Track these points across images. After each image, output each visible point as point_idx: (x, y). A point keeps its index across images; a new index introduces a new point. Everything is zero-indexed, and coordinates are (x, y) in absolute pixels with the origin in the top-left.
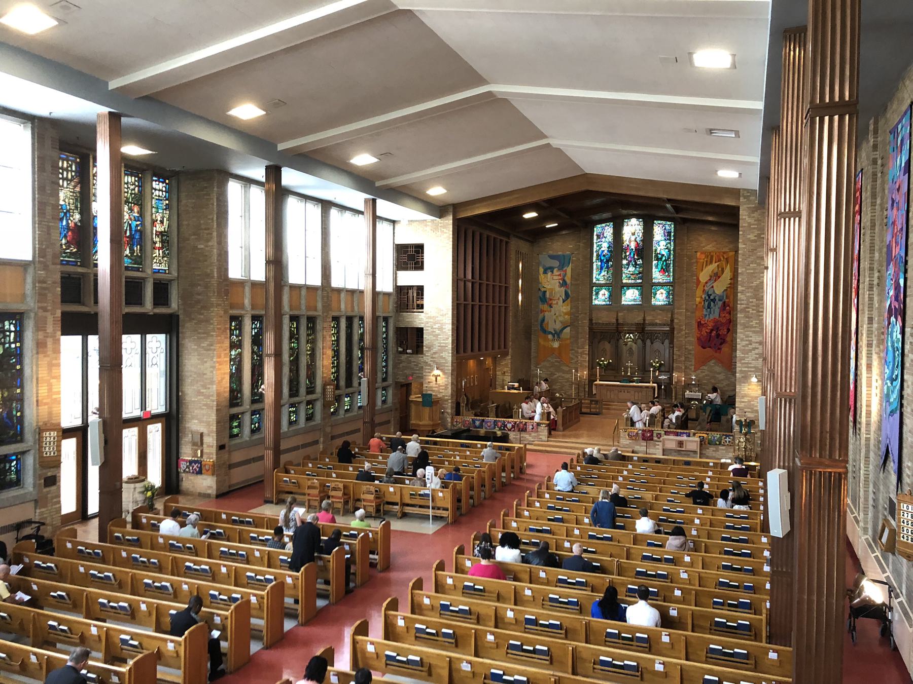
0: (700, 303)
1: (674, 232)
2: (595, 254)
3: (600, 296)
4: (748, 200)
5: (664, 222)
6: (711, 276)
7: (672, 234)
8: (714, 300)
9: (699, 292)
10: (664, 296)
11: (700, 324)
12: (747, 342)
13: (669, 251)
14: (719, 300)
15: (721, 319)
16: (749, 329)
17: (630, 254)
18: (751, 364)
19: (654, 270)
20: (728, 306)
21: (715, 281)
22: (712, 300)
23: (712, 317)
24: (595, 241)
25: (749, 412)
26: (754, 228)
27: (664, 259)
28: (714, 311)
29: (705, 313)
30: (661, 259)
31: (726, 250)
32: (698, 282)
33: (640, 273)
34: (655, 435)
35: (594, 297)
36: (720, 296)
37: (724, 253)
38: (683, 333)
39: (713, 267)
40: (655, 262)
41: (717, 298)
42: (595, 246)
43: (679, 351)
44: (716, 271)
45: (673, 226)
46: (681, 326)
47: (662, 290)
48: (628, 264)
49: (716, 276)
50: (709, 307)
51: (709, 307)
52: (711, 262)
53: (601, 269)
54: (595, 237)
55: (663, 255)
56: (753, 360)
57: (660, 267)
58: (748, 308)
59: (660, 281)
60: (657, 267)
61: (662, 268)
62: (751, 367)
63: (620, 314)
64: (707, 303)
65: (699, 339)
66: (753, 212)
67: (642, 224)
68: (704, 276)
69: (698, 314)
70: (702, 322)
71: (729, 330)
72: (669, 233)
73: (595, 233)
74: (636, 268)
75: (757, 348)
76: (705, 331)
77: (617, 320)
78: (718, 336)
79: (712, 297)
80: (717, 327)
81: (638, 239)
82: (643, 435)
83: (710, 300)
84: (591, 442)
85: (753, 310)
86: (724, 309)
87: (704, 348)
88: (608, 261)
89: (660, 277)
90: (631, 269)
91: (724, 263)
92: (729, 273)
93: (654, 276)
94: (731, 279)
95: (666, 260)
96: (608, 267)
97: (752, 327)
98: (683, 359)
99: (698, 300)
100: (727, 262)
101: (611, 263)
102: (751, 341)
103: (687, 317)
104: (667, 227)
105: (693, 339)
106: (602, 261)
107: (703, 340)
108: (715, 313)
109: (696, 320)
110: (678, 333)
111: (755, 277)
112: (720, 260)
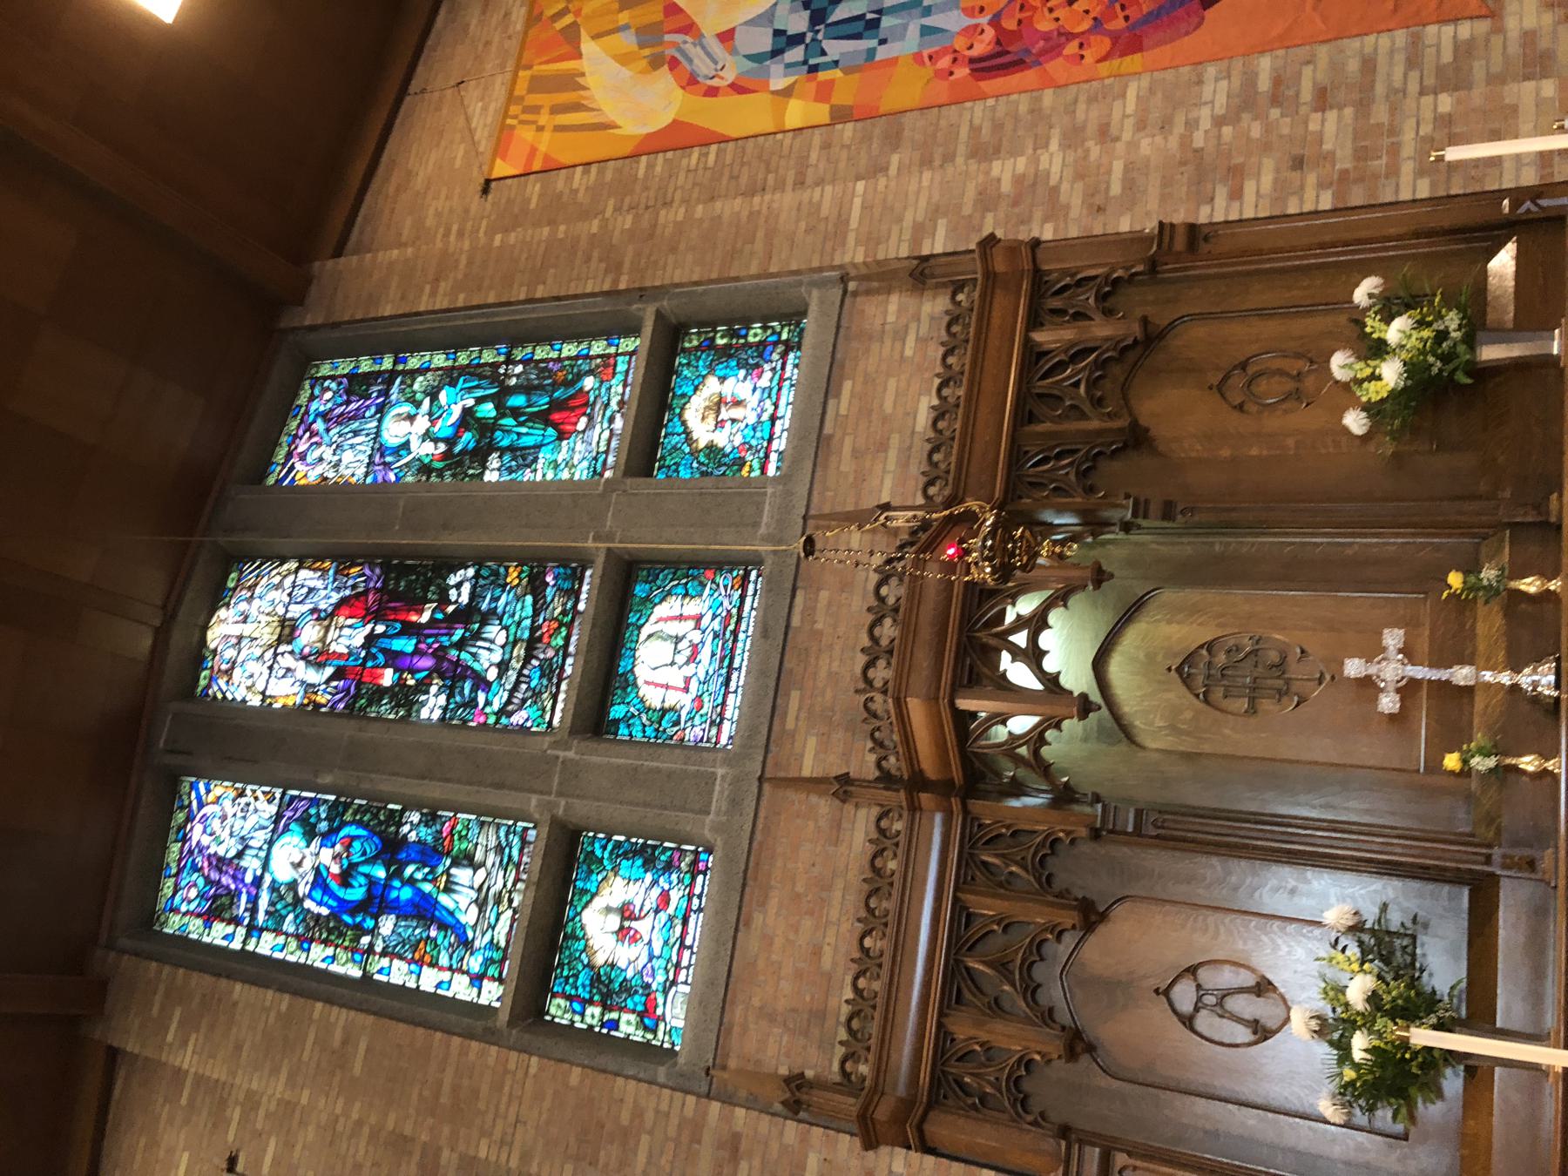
0: (824, 93)
1: (354, 352)
2: (318, 955)
3: (627, 957)
6: (655, 63)
7: (366, 365)
10: (737, 385)
13: (450, 376)
17: (394, 658)
19: (541, 472)
22: (817, 18)
27: (487, 410)
30: (486, 429)
33: (536, 587)
35: (628, 1027)
38: (1054, 161)
42: (266, 945)
43: (1236, 176)
44: (627, 41)
47: (692, 414)
48: (454, 675)
53: (424, 911)
54: (218, 934)
57: (530, 436)
60: (524, 456)
61: (543, 418)
63: (808, 768)
64: (835, 48)
72: (356, 385)
73: (195, 929)
74: (485, 619)
88: (392, 850)
93: (582, 473)
95: (499, 400)
101: (413, 829)
106: (377, 902)
109: (958, 99)
110: (1055, 209)
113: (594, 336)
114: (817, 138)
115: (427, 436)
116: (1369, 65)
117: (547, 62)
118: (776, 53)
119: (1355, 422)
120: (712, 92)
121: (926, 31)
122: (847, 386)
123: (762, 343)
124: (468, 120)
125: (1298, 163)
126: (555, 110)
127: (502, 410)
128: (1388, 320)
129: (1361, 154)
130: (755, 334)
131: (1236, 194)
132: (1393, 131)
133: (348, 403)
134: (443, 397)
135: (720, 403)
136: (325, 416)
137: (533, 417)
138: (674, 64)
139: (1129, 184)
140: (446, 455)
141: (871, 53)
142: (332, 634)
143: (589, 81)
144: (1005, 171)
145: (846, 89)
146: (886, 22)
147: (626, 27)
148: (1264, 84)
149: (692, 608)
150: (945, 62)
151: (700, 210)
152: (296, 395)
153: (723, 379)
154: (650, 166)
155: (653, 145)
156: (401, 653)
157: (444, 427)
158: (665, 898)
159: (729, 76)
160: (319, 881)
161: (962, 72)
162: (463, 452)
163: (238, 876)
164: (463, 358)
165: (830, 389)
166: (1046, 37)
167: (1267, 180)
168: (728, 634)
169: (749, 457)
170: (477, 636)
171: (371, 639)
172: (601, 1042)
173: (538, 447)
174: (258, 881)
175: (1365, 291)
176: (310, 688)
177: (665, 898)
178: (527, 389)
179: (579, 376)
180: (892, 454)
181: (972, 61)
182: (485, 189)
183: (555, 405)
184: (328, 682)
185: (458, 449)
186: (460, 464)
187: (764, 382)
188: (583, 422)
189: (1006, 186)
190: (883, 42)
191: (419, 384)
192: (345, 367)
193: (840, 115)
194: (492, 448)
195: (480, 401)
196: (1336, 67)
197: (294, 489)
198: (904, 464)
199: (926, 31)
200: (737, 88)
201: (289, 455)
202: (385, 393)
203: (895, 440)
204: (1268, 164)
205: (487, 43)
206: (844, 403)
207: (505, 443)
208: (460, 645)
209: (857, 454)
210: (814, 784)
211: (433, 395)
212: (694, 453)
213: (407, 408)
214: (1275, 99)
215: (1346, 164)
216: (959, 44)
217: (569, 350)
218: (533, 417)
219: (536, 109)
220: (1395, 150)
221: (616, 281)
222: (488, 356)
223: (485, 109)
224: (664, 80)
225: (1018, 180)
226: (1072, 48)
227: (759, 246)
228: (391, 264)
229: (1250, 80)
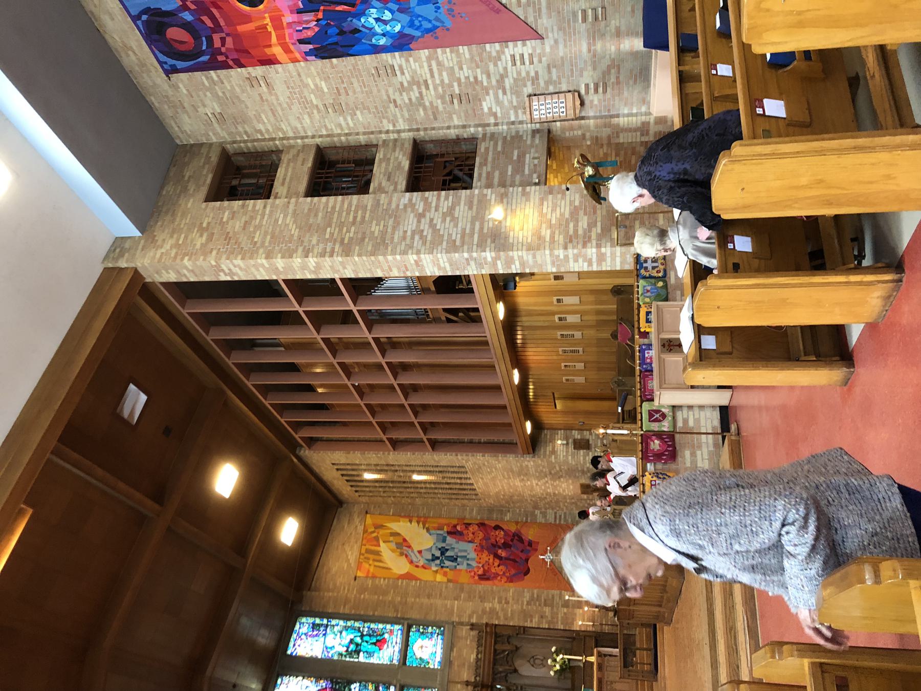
0: (445, 574)
1: (315, 617)
4: (129, 250)
5: (294, 636)
6: (401, 554)
8: (443, 551)
9: (426, 575)
12: (417, 237)
14: (444, 540)
15: (477, 540)
16: (388, 236)
18: (464, 230)
19: (374, 660)
20: (455, 526)
21: (409, 547)
22: (442, 554)
23: (473, 555)
25: (576, 226)
26: (186, 238)
27: (358, 640)
28: (461, 551)
29: (463, 567)
30: (357, 645)
31: (361, 529)
32: (408, 576)
34: (655, 427)
36: (438, 540)
37: (365, 531)
38: (497, 606)
39: (386, 550)
40: (362, 658)
41: (440, 545)
43: (531, 617)
44: (393, 546)
45: (304, 620)
46: (484, 612)
49: (403, 546)
50: (454, 559)
51: (454, 559)
52: (378, 553)
55: (351, 641)
56: (456, 226)
58: (342, 240)
59: (397, 649)
60: (370, 654)
61: (375, 644)
62: (473, 229)
64: (447, 563)
65: (511, 580)
66: (153, 240)
67: (286, 679)
68: (398, 565)
69: (464, 578)
70: (480, 572)
71: (497, 527)
72: (315, 626)
75: (432, 220)
76: (497, 568)
78: (506, 546)
79: (438, 554)
80: (492, 548)
82: (658, 456)
83: (442, 556)
84: (704, 606)
85: (348, 231)
86: (461, 534)
87: (527, 572)
89: (390, 650)
91: (382, 532)
92: (401, 523)
93: (386, 661)
94: (411, 521)
95: (362, 636)
97: (383, 233)
98: (547, 610)
99: (439, 578)
102: (413, 233)
103: (470, 598)
104: (304, 630)
105: (511, 590)
107: (513, 572)
108: (467, 549)
109: (476, 583)
110: (498, 618)
111: (281, 231)
112: (377, 539)
113: (387, 623)
114: (444, 585)
116: (553, 596)
117: (372, 545)
118: (433, 560)
119: (552, 673)
120: (417, 566)
121: (468, 565)
122: (455, 649)
123: (432, 633)
124: (347, 556)
125: (542, 617)
126: (374, 560)
127: (363, 641)
128: (557, 655)
129: (553, 618)
130: (430, 629)
131: (531, 621)
132: (558, 614)
134: (344, 633)
135: (422, 647)
136: (306, 634)
137: (372, 644)
138: (406, 556)
139: (512, 614)
140: (347, 651)
141: (456, 567)
143: (383, 554)
144: (488, 606)
145: (451, 574)
146: (459, 559)
147: (391, 542)
148: (535, 596)
150: (472, 574)
151: (418, 600)
154: (402, 583)
157: (346, 641)
159: (421, 563)
161: (477, 578)
162: (352, 651)
164: (349, 623)
165: (451, 650)
166: (494, 574)
167: (537, 619)
169: (430, 661)
173: (374, 652)
175: (553, 649)
178: (370, 636)
179: (383, 634)
180: (466, 667)
181: (479, 575)
182: (355, 579)
183: (378, 641)
185: (350, 650)
186: (351, 654)
188: (386, 646)
189: (488, 609)
191: (336, 629)
192: (311, 620)
193: (449, 581)
194: (360, 651)
196: (548, 595)
197: (296, 656)
198: (468, 669)
199: (468, 565)
200: (424, 567)
201: (294, 645)
202: (326, 630)
203: (467, 664)
204: (537, 616)
205: (351, 534)
206: (454, 654)
207: (364, 650)
209: (458, 666)
211: (341, 633)
212: (417, 659)
213: (333, 636)
214: (537, 600)
215: (550, 619)
217: (381, 626)
218: (372, 644)
219: (368, 559)
220: (558, 618)
221: (397, 614)
222: (357, 624)
223: (352, 554)
224: (403, 560)
225: (490, 608)
226: (499, 578)
227: (433, 611)
228: (330, 597)
229: (533, 594)
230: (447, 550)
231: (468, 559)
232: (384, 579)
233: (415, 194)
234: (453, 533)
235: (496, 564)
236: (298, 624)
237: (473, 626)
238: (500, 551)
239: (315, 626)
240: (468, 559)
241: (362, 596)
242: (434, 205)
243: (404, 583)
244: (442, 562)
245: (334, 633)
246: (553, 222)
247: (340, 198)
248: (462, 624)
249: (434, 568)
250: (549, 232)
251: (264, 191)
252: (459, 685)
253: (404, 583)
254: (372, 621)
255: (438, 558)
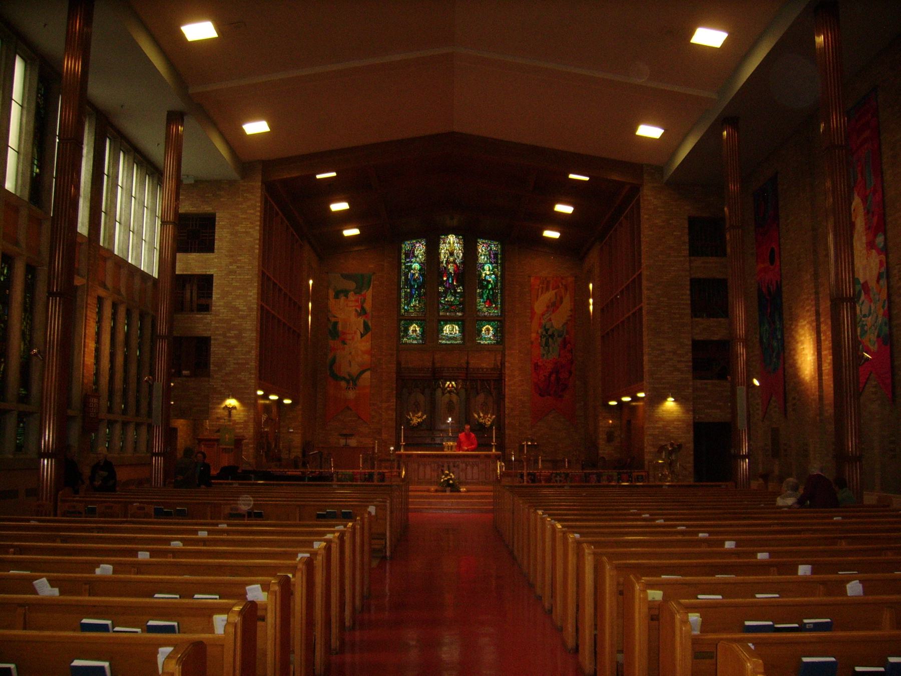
0: (537, 339)
6: (548, 307)
7: (499, 256)
8: (552, 336)
11: (536, 366)
13: (496, 276)
14: (559, 336)
17: (448, 279)
21: (553, 311)
22: (550, 336)
24: (403, 261)
27: (490, 286)
30: (487, 286)
32: (533, 313)
35: (402, 334)
39: (549, 295)
45: (499, 247)
48: (445, 292)
49: (554, 306)
50: (547, 344)
52: (547, 289)
53: (412, 296)
54: (403, 256)
55: (489, 282)
61: (488, 298)
64: (544, 340)
68: (539, 306)
70: (539, 364)
72: (496, 255)
74: (455, 297)
77: (433, 363)
81: (458, 261)
90: (450, 298)
91: (563, 291)
94: (571, 310)
95: (492, 289)
96: (419, 295)
99: (534, 335)
100: (566, 290)
106: (412, 287)
112: (557, 287)
115: (486, 274)
118: (545, 330)
120: (540, 319)
121: (544, 355)
123: (497, 336)
127: (489, 290)
133: (493, 254)
134: (493, 276)
136: (491, 249)
138: (547, 311)
141: (542, 346)
142: (452, 264)
149: (457, 332)
152: (495, 241)
153: (493, 331)
155: (532, 309)
156: (449, 281)
157: (488, 277)
158: (418, 336)
160: (414, 274)
163: (412, 258)
164: (499, 278)
168: (454, 338)
170: (452, 295)
171: (451, 273)
172: (399, 330)
174: (412, 262)
176: (442, 262)
177: (418, 336)
181: (537, 363)
184: (444, 266)
187: (492, 338)
190: (544, 348)
193: (532, 343)
195: (492, 284)
199: (544, 355)
202: (494, 263)
207: (484, 292)
208: (451, 292)
210: (434, 359)
216: (541, 360)
217: (499, 300)
222: (499, 284)
230: (553, 339)
231: (547, 354)
232: (530, 300)
233: (690, 347)
234: (565, 343)
235: (545, 374)
236: (497, 243)
237: (503, 364)
238: (554, 375)
239: (496, 255)
240: (547, 354)
241: (517, 286)
242: (682, 359)
243: (528, 314)
244: (545, 336)
245: (493, 269)
246: (667, 428)
247: (689, 302)
248: (503, 355)
249: (540, 331)
250: (661, 426)
251: (695, 251)
252: (466, 358)
253: (528, 314)
254: (501, 296)
255: (547, 333)
